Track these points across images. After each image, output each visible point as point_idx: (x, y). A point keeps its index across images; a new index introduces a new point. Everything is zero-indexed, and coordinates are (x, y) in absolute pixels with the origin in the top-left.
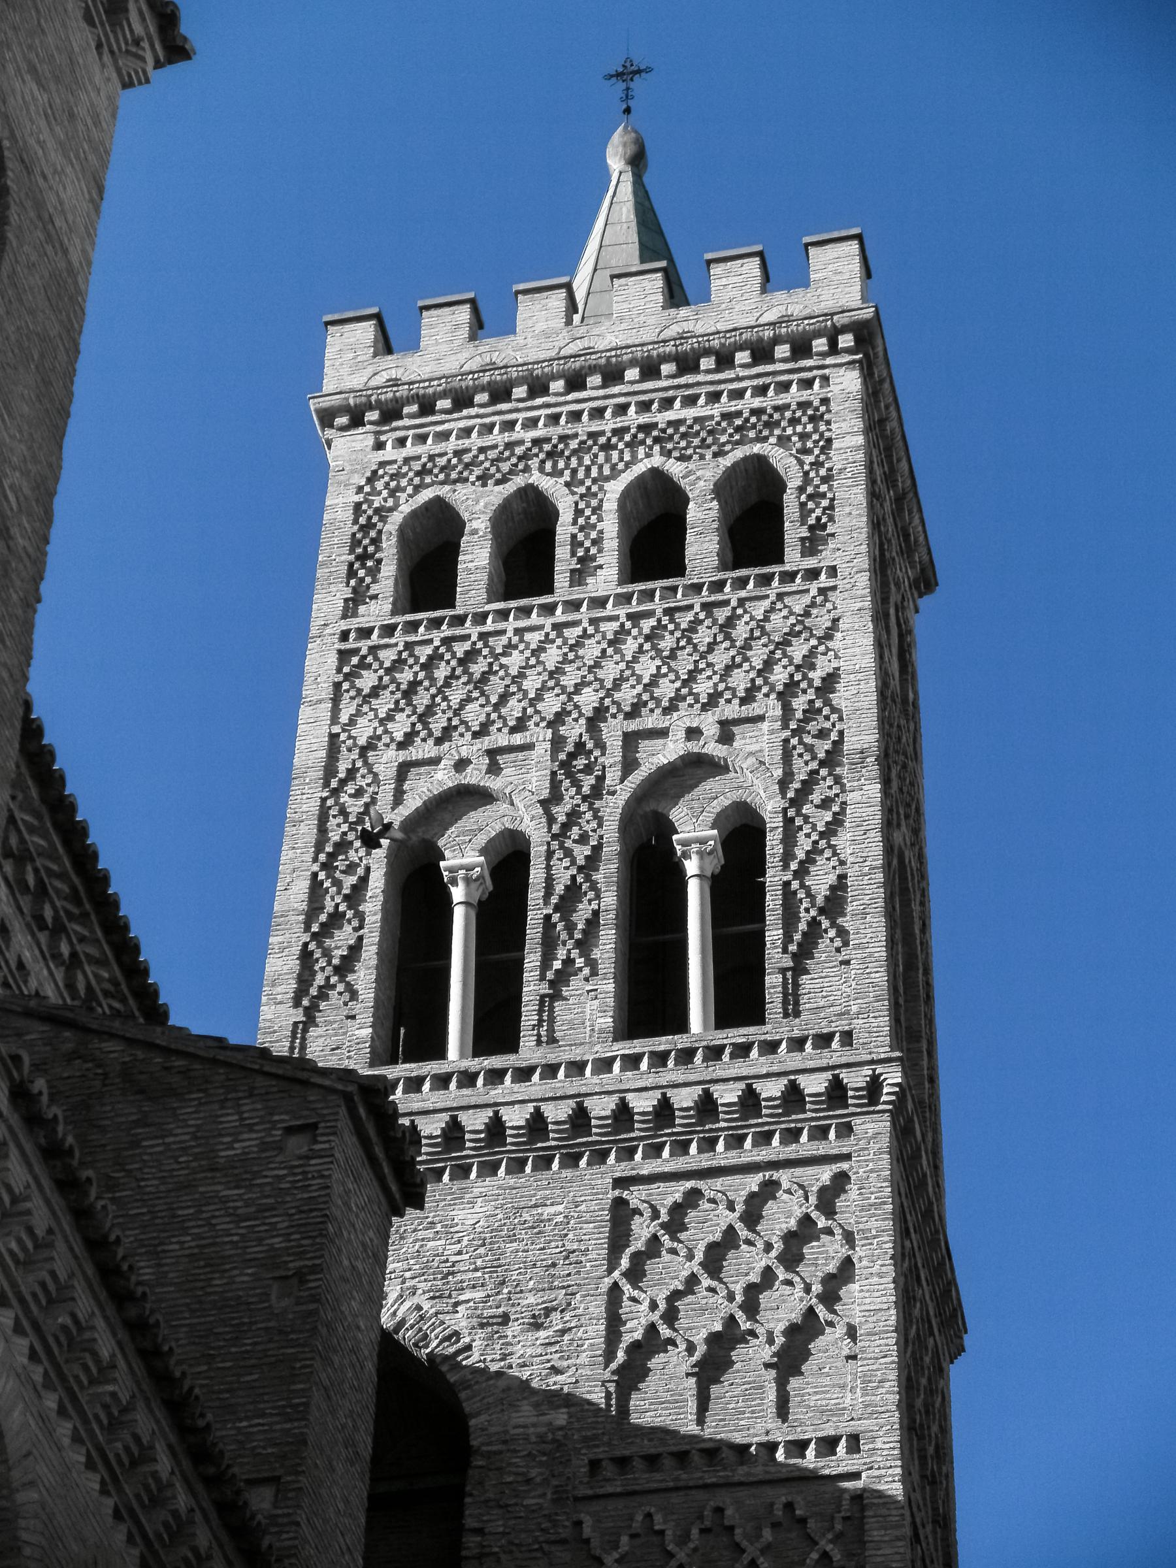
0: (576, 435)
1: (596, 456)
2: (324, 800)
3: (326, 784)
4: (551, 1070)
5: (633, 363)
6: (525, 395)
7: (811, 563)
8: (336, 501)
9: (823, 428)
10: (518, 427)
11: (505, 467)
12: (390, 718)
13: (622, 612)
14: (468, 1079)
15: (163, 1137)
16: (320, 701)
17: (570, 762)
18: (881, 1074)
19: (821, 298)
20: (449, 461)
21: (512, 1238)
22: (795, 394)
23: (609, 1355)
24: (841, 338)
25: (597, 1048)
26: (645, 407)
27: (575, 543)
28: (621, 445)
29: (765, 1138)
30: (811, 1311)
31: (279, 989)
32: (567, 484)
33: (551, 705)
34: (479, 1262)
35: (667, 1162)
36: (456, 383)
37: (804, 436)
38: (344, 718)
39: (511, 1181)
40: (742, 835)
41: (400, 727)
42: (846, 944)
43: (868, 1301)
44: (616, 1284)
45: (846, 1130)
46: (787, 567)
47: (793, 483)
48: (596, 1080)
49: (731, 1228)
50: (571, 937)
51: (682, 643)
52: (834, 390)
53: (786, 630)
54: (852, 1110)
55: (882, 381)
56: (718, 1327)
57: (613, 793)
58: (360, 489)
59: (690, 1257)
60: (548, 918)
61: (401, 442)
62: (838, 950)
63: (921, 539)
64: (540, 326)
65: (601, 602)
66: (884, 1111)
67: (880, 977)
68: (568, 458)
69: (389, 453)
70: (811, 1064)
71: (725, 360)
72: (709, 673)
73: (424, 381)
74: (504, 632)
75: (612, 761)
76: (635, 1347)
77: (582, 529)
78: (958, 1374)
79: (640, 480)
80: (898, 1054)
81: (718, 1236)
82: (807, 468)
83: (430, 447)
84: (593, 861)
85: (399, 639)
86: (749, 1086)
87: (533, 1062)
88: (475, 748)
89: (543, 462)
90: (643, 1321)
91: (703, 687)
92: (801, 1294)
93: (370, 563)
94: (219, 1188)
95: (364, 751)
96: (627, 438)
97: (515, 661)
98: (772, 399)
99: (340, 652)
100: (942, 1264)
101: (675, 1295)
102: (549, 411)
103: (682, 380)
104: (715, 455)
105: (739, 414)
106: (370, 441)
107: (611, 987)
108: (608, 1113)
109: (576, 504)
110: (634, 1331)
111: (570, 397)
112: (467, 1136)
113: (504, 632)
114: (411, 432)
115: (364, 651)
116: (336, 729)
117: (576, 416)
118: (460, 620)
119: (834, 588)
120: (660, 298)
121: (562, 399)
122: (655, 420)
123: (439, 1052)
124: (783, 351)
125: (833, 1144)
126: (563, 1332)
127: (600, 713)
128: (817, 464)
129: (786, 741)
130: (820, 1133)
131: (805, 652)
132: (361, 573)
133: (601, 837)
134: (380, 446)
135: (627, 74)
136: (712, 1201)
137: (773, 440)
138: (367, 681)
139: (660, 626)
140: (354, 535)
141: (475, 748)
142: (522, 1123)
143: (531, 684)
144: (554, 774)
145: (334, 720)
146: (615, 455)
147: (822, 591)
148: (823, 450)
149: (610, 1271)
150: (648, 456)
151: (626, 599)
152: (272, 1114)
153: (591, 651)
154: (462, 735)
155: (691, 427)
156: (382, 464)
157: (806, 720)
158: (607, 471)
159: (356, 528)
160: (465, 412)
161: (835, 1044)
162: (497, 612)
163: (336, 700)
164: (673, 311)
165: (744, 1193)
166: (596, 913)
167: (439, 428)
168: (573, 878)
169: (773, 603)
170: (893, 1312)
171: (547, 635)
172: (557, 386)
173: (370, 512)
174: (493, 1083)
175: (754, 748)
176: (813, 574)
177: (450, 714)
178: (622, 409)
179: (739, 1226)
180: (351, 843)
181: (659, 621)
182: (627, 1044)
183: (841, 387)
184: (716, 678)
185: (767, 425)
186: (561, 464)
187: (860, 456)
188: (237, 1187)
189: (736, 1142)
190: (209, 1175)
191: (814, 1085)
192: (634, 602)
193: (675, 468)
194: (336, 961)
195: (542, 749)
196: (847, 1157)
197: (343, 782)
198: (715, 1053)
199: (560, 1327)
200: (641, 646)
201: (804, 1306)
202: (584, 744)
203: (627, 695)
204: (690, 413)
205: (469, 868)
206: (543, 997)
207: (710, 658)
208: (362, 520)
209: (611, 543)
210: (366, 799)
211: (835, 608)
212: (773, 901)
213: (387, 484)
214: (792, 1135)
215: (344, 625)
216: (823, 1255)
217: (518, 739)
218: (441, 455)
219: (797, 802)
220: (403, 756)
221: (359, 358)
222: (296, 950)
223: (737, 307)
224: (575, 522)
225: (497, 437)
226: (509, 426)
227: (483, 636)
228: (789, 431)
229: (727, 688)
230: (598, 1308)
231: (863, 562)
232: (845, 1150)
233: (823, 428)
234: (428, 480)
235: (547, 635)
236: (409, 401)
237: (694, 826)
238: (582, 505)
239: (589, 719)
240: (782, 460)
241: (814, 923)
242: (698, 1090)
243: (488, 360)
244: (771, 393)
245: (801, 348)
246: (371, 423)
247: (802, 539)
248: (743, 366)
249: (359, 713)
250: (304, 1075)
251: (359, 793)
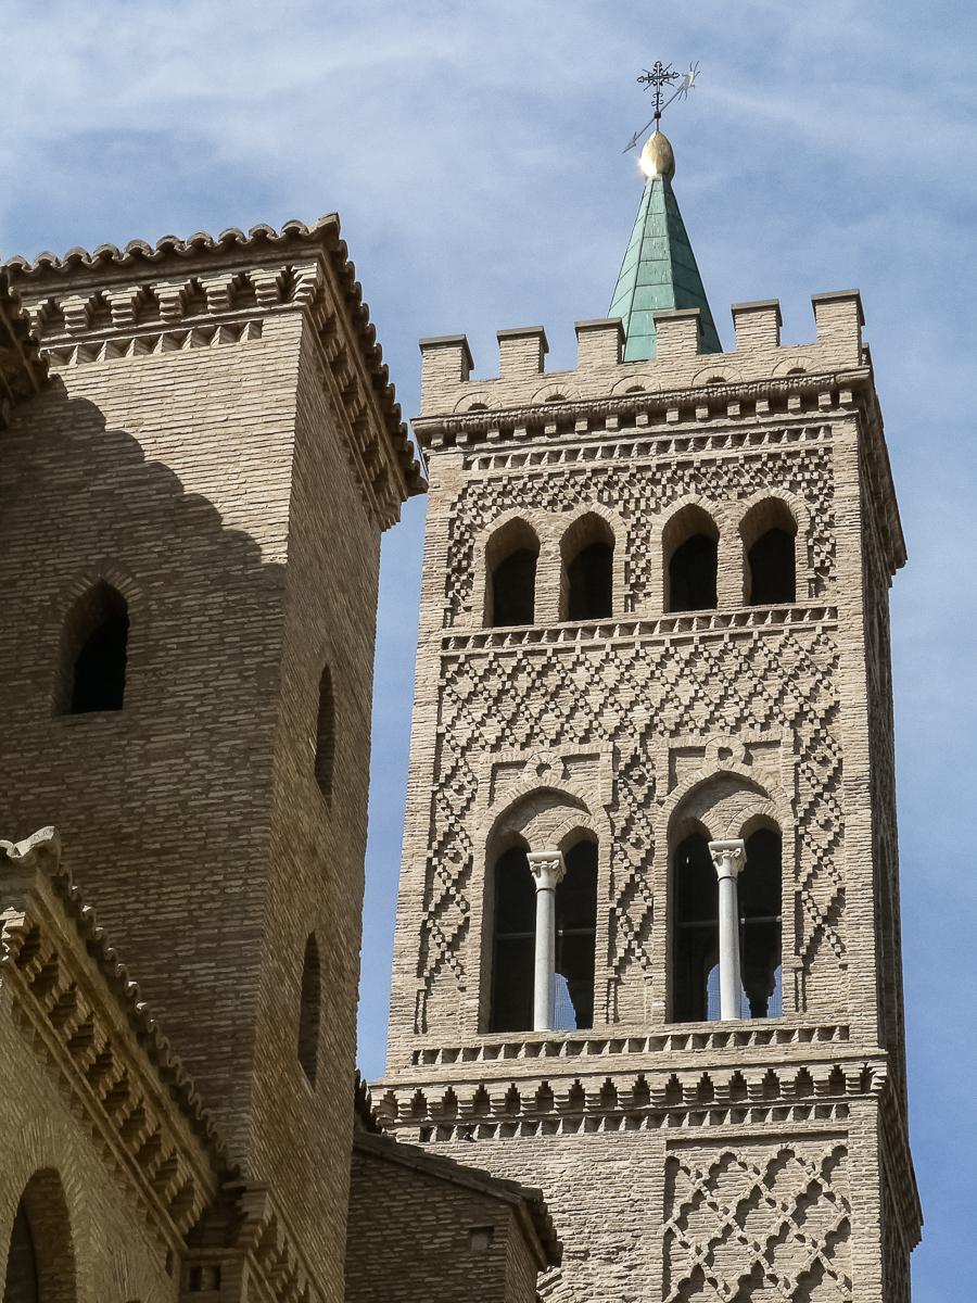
0: (627, 468)
1: (644, 489)
2: (434, 793)
3: (436, 779)
4: (617, 1045)
5: (674, 405)
6: (585, 428)
7: (816, 603)
8: (435, 516)
9: (826, 476)
10: (580, 457)
11: (571, 493)
12: (482, 723)
13: (667, 638)
14: (554, 1048)
15: (381, 1230)
16: (428, 703)
17: (629, 770)
18: (871, 1068)
19: (826, 354)
20: (525, 484)
21: (591, 1187)
22: (804, 443)
23: (666, 1289)
24: (841, 395)
25: (652, 1028)
26: (682, 445)
27: (628, 571)
28: (664, 481)
29: (781, 1114)
30: (817, 1261)
31: (406, 961)
32: (621, 514)
33: (611, 719)
34: (566, 1207)
35: (706, 1129)
36: (529, 414)
37: (811, 482)
38: (447, 720)
39: (589, 1137)
40: (762, 840)
41: (491, 732)
42: (843, 950)
43: (859, 1256)
44: (670, 1230)
45: (844, 1111)
46: (797, 606)
47: (803, 527)
48: (653, 1055)
49: (757, 1187)
50: (631, 930)
51: (715, 670)
52: (836, 439)
53: (797, 664)
54: (847, 1095)
55: (872, 422)
56: (748, 1271)
57: (661, 803)
58: (454, 504)
59: (726, 1211)
60: (613, 911)
61: (485, 462)
62: (838, 955)
63: (897, 530)
64: (598, 363)
65: (648, 627)
66: (872, 1098)
67: (871, 981)
68: (622, 489)
69: (476, 472)
70: (817, 1055)
71: (747, 407)
72: (737, 699)
73: (505, 411)
74: (573, 649)
75: (661, 774)
76: (684, 1284)
77: (634, 557)
78: (915, 1257)
79: (680, 513)
80: (883, 1052)
81: (746, 1194)
82: (813, 514)
83: (508, 469)
84: (647, 861)
85: (489, 648)
86: (770, 1071)
87: (604, 1037)
88: (553, 755)
89: (601, 491)
90: (692, 1264)
91: (731, 712)
92: (811, 1247)
93: (464, 577)
94: (425, 1275)
95: (464, 749)
96: (669, 474)
97: (582, 676)
98: (784, 446)
99: (443, 658)
100: (908, 1189)
101: (714, 1243)
102: (606, 444)
103: (713, 423)
104: (741, 495)
105: (758, 457)
106: (461, 462)
107: (663, 976)
108: (663, 1087)
109: (629, 533)
110: (682, 1270)
111: (624, 431)
112: (555, 1100)
113: (573, 649)
114: (493, 455)
115: (462, 660)
116: (442, 730)
117: (627, 449)
118: (536, 636)
119: (834, 628)
120: (694, 343)
121: (615, 434)
122: (691, 458)
123: (528, 1025)
124: (794, 403)
125: (833, 1123)
126: (631, 1268)
127: (650, 727)
128: (822, 510)
129: (797, 765)
130: (824, 1112)
131: (812, 685)
132: (457, 586)
133: (653, 842)
134: (467, 465)
135: (658, 77)
136: (743, 1165)
137: (786, 485)
138: (464, 685)
139: (696, 654)
140: (450, 548)
141: (553, 755)
142: (598, 1092)
143: (595, 698)
144: (615, 782)
145: (439, 723)
146: (658, 490)
147: (825, 629)
148: (829, 495)
149: (666, 1219)
150: (686, 492)
151: (671, 624)
152: (460, 1217)
153: (641, 672)
154: (542, 742)
155: (720, 467)
156: (471, 483)
157: (811, 748)
158: (653, 506)
159: (452, 542)
160: (536, 440)
161: (836, 1037)
162: (567, 630)
163: (440, 702)
164: (705, 357)
165: (767, 1159)
166: (650, 909)
167: (516, 453)
168: (632, 877)
169: (787, 638)
170: (880, 1266)
171: (608, 654)
172: (612, 422)
173: (463, 529)
174: (573, 1054)
175: (772, 768)
176: (818, 613)
177: (532, 722)
178: (664, 446)
179: (763, 1187)
180: (458, 833)
181: (696, 648)
182: (676, 1026)
183: (841, 438)
184: (742, 704)
185: (781, 468)
186: (616, 496)
187: (856, 505)
188: (437, 1275)
189: (760, 1115)
190: (416, 1264)
191: (820, 1073)
192: (676, 630)
193: (708, 506)
194: (449, 939)
195: (606, 758)
196: (844, 1134)
197: (449, 778)
198: (743, 1038)
199: (628, 1264)
200: (682, 670)
201: (812, 1257)
202: (639, 757)
203: (671, 714)
204: (719, 454)
205: (550, 860)
206: (610, 980)
207: (736, 685)
208: (457, 536)
209: (658, 573)
210: (467, 794)
211: (836, 646)
212: (788, 908)
213: (475, 502)
214: (802, 1113)
215: (445, 633)
216: (823, 1216)
217: (586, 749)
218: (518, 478)
219: (804, 821)
220: (497, 757)
221: (450, 382)
222: (418, 927)
223: (758, 357)
224: (628, 551)
225: (562, 465)
226: (573, 454)
227: (556, 652)
228: (799, 478)
229: (751, 714)
230: (658, 1251)
231: (858, 606)
232: (843, 1128)
233: (826, 476)
234: (507, 501)
235: (608, 654)
236: (491, 426)
237: (724, 829)
238: (633, 536)
239: (641, 734)
240: (797, 503)
241: (819, 930)
242: (730, 1073)
243: (554, 393)
244: (784, 440)
245: (809, 401)
246: (460, 444)
247: (810, 581)
248: (761, 414)
249: (457, 718)
250: (482, 1187)
251: (460, 791)
